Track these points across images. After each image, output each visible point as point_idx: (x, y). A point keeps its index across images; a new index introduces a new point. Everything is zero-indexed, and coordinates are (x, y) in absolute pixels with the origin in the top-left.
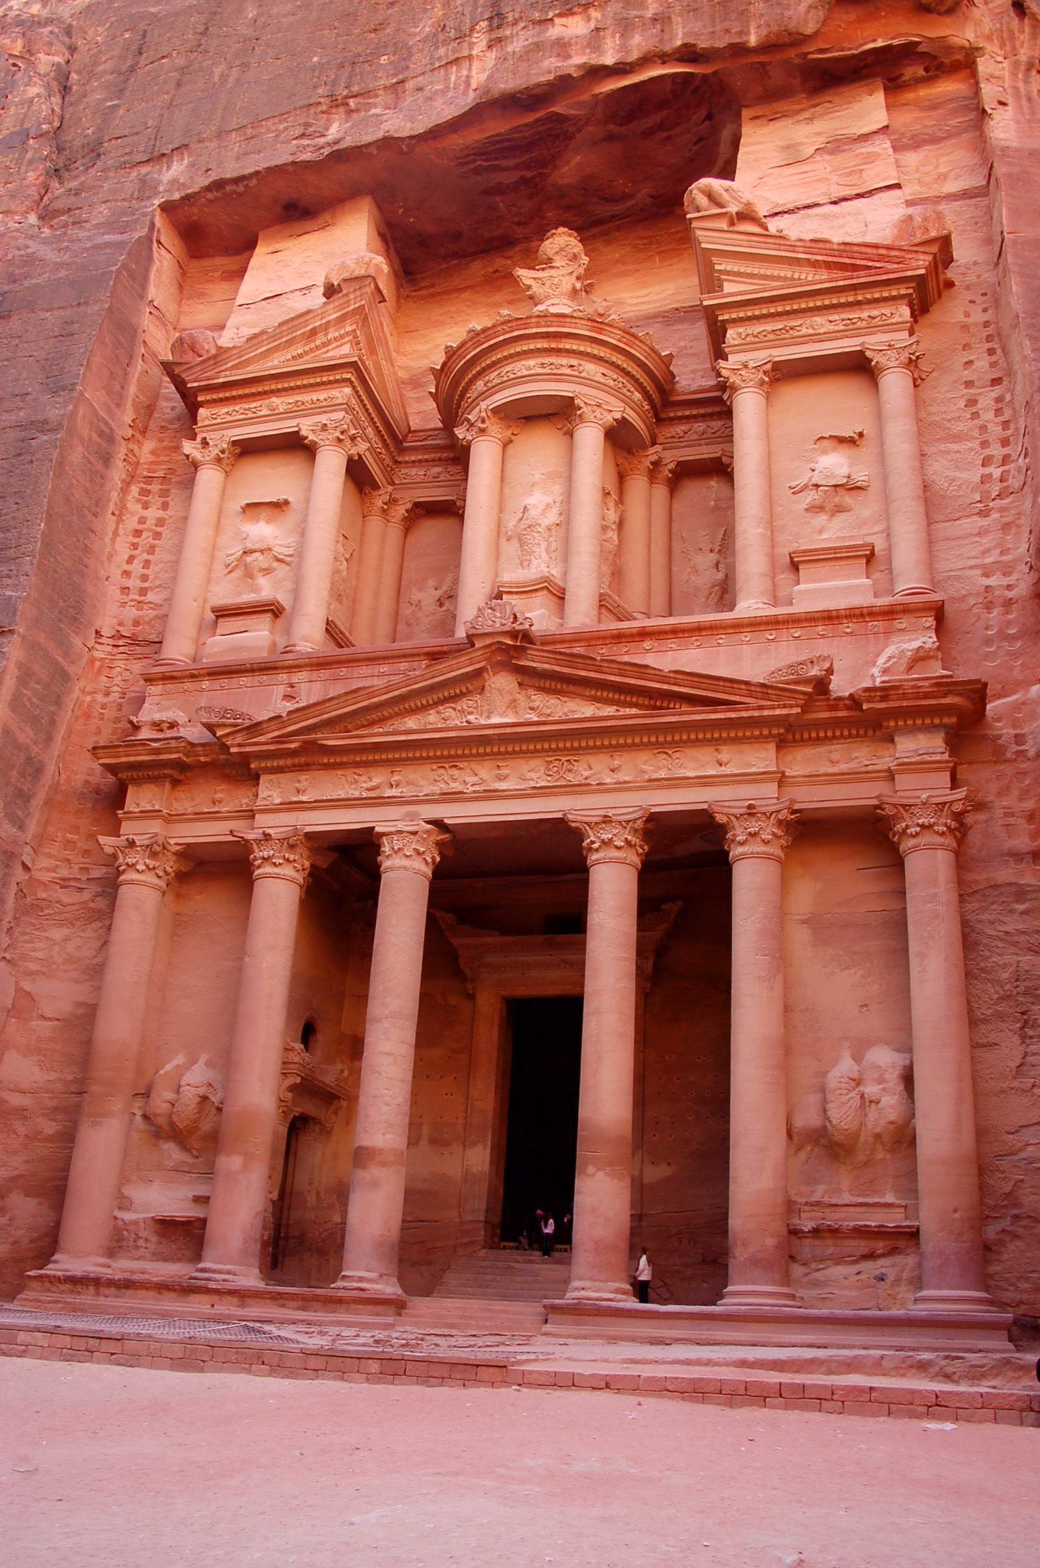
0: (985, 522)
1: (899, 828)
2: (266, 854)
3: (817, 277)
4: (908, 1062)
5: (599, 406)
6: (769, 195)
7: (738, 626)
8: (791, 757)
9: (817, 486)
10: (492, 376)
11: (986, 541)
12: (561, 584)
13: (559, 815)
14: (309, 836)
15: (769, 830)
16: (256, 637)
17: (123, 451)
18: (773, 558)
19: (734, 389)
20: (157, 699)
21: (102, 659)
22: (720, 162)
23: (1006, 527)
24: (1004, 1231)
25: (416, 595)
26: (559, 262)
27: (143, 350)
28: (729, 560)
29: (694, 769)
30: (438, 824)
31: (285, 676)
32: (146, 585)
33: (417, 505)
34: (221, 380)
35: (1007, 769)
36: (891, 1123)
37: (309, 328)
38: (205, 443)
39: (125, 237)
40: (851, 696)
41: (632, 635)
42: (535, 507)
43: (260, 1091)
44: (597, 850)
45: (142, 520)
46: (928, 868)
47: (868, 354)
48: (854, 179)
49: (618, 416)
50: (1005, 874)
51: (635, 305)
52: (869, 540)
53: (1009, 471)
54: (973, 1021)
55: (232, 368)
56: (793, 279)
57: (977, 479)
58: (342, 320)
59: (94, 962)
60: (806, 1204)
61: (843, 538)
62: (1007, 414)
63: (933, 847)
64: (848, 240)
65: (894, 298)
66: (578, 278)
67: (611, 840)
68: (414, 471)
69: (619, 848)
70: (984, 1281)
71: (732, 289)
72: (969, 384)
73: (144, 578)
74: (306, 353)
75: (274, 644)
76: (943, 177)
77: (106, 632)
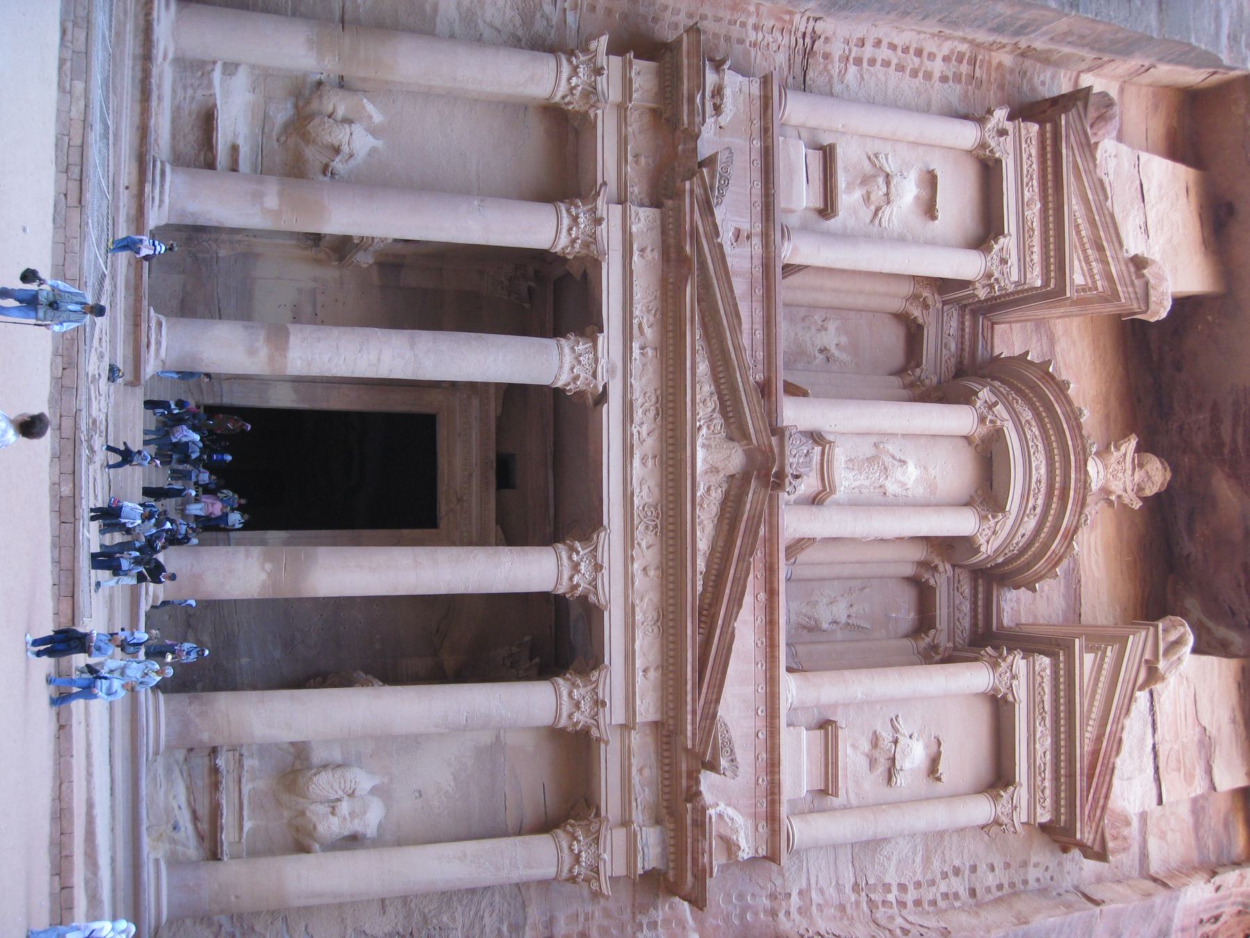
0: (848, 889)
1: (580, 834)
2: (581, 220)
3: (1087, 741)
4: (369, 835)
5: (994, 533)
6: (1171, 687)
7: (772, 682)
9: (896, 742)
10: (1036, 430)
11: (831, 892)
12: (829, 500)
13: (605, 522)
14: (597, 264)
15: (582, 718)
16: (799, 194)
17: (1005, 41)
18: (835, 706)
20: (746, 90)
21: (791, 22)
22: (1211, 624)
23: (842, 908)
24: (221, 926)
25: (832, 326)
26: (1138, 475)
27: (1105, 59)
28: (839, 636)
29: (641, 646)
30: (602, 398)
31: (759, 230)
32: (865, 64)
33: (920, 328)
34: (1064, 151)
35: (627, 916)
36: (315, 827)
37: (1105, 244)
38: (1002, 133)
39: (1224, 40)
40: (700, 793)
41: (771, 582)
42: (904, 473)
43: (345, 217)
44: (570, 558)
45: (932, 56)
46: (539, 857)
47: (1011, 788)
48: (1173, 763)
49: (983, 549)
50: (534, 914)
51: (1089, 540)
52: (842, 792)
53: (891, 908)
54: (405, 899)
55: (1075, 162)
56: (1089, 718)
57: (886, 881)
58: (1109, 277)
59: (480, 21)
60: (241, 755)
61: (845, 769)
62: (942, 904)
63: (560, 862)
64: (1116, 772)
66: (1119, 497)
67: (579, 571)
68: (954, 324)
69: (571, 578)
70: (176, 919)
71: (1087, 662)
72: (974, 869)
73: (872, 62)
74: (1080, 238)
75: (792, 211)
76: (1163, 836)
77: (820, 26)
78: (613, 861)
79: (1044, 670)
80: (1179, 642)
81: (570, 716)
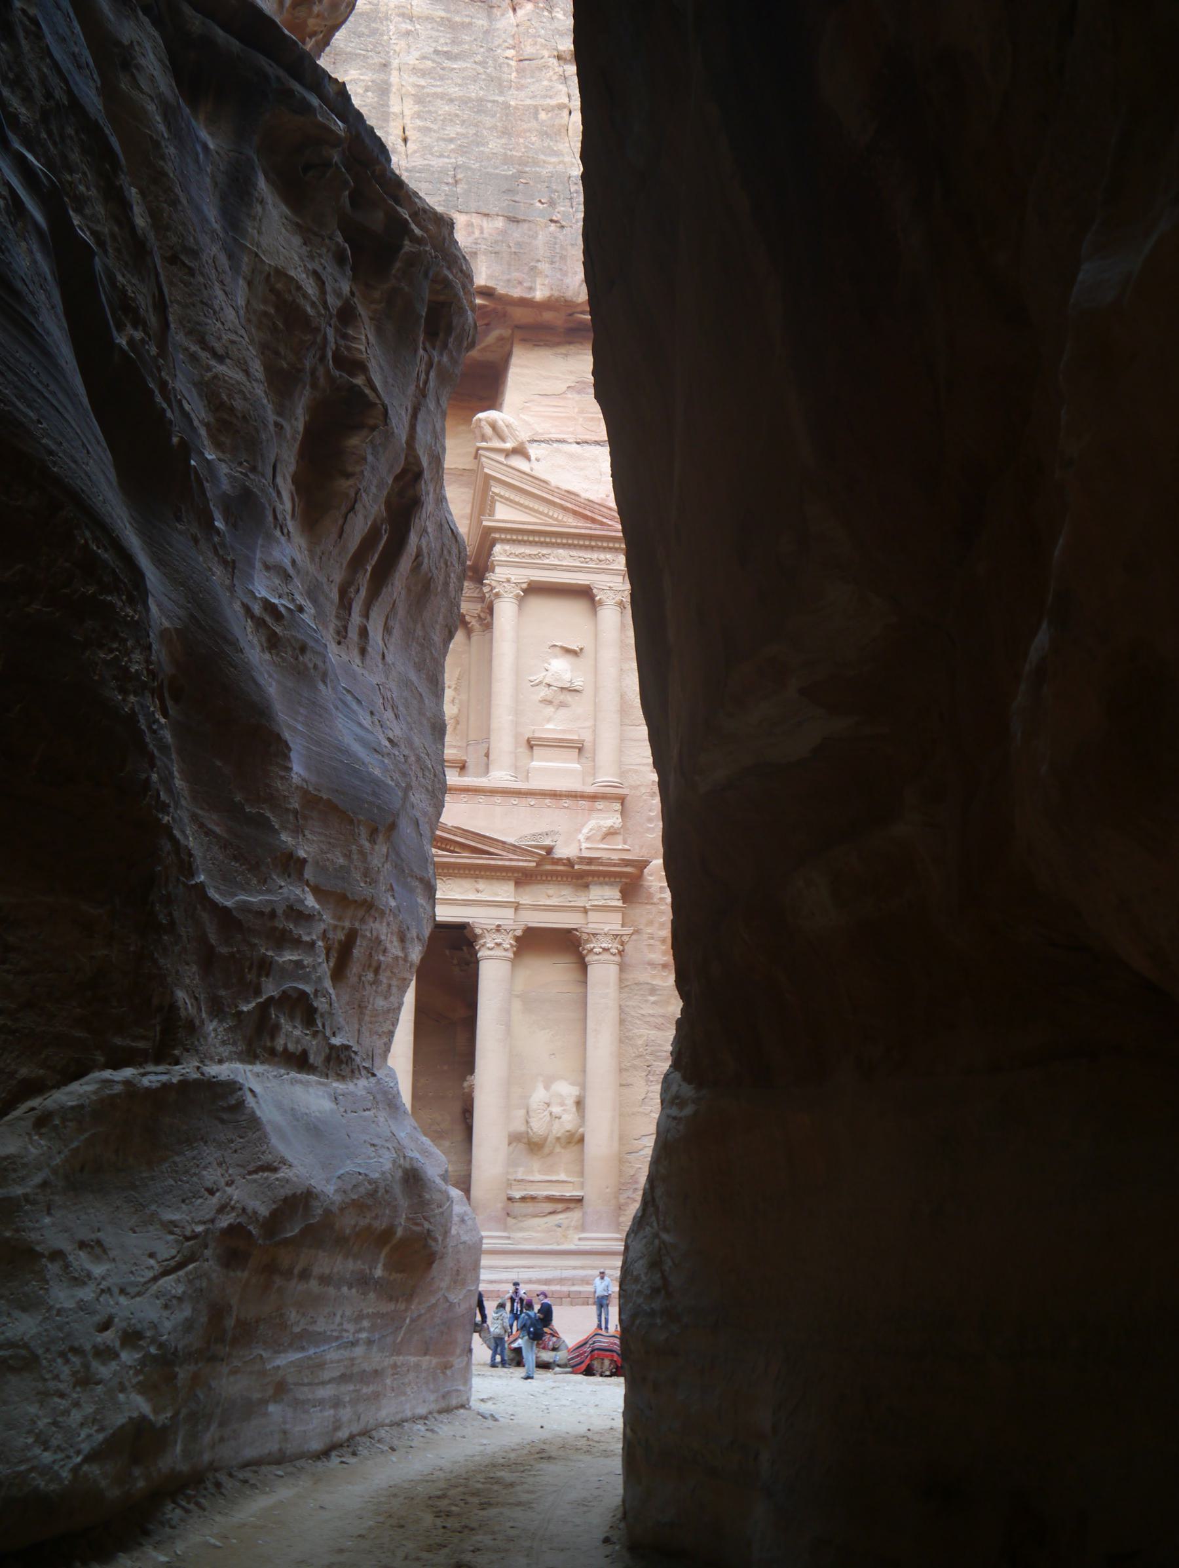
8: (521, 890)
9: (549, 685)
15: (508, 941)
18: (517, 736)
19: (498, 595)
35: (653, 909)
40: (568, 859)
46: (602, 973)
47: (595, 591)
50: (645, 976)
54: (621, 1070)
56: (547, 515)
61: (564, 731)
63: (608, 962)
64: (592, 498)
65: (616, 549)
78: (610, 923)
79: (505, 551)
80: (494, 426)
81: (506, 950)
